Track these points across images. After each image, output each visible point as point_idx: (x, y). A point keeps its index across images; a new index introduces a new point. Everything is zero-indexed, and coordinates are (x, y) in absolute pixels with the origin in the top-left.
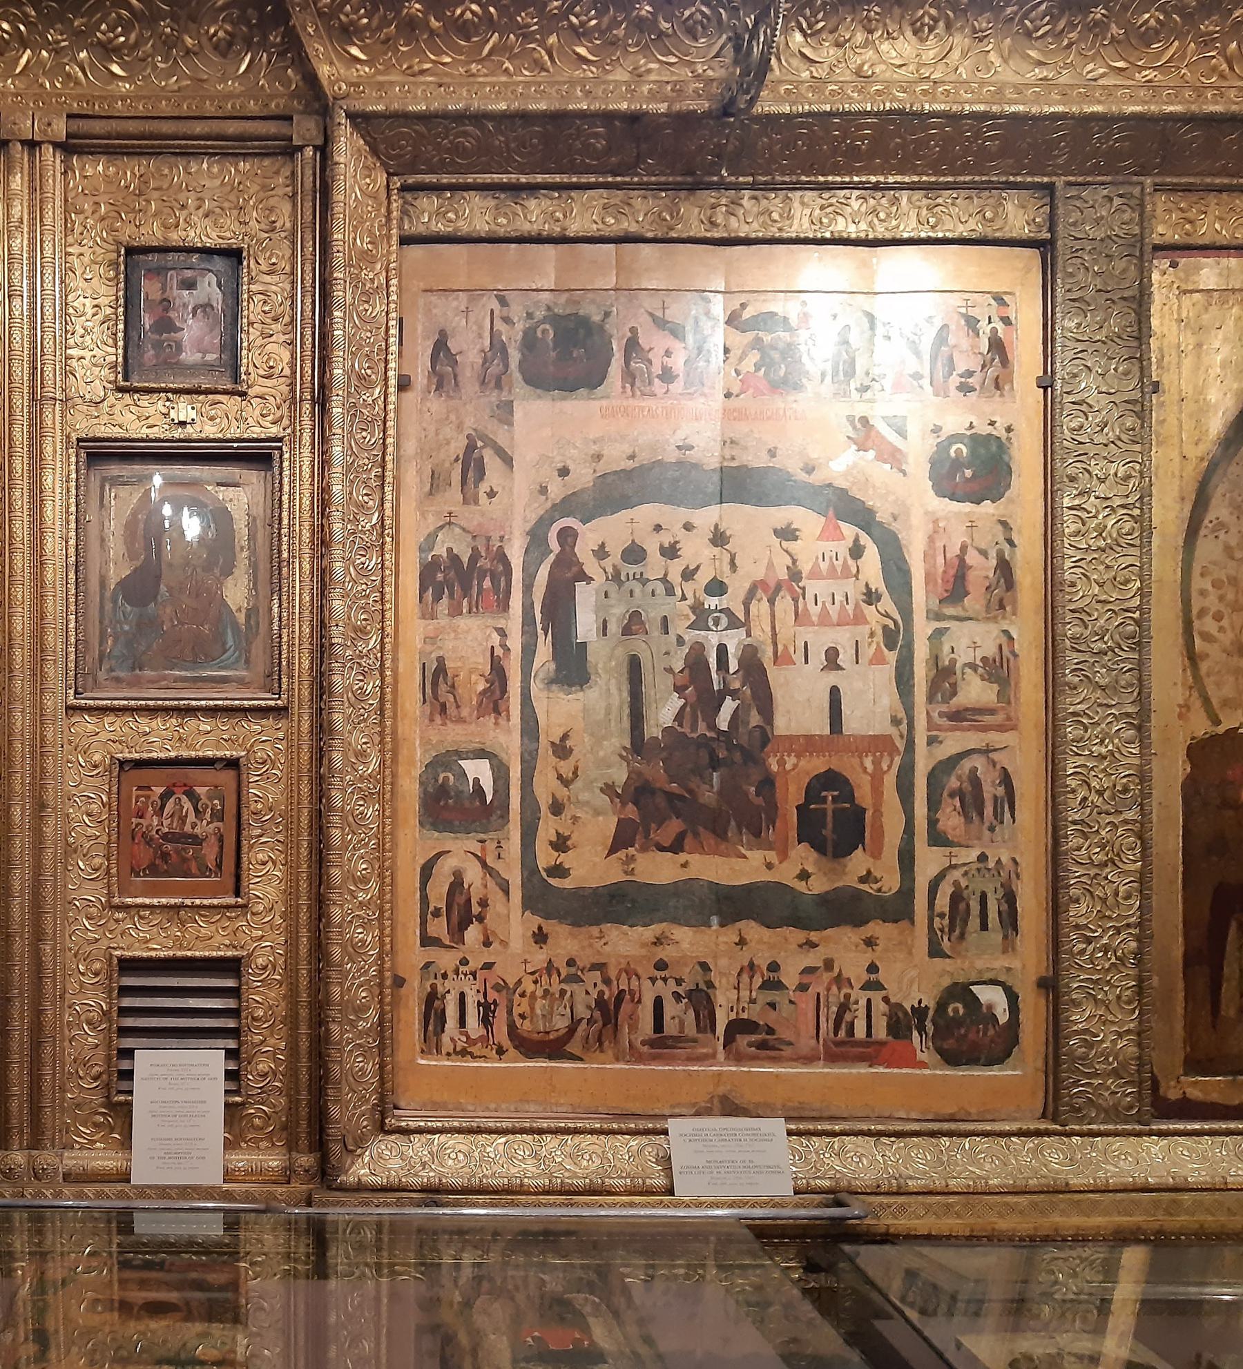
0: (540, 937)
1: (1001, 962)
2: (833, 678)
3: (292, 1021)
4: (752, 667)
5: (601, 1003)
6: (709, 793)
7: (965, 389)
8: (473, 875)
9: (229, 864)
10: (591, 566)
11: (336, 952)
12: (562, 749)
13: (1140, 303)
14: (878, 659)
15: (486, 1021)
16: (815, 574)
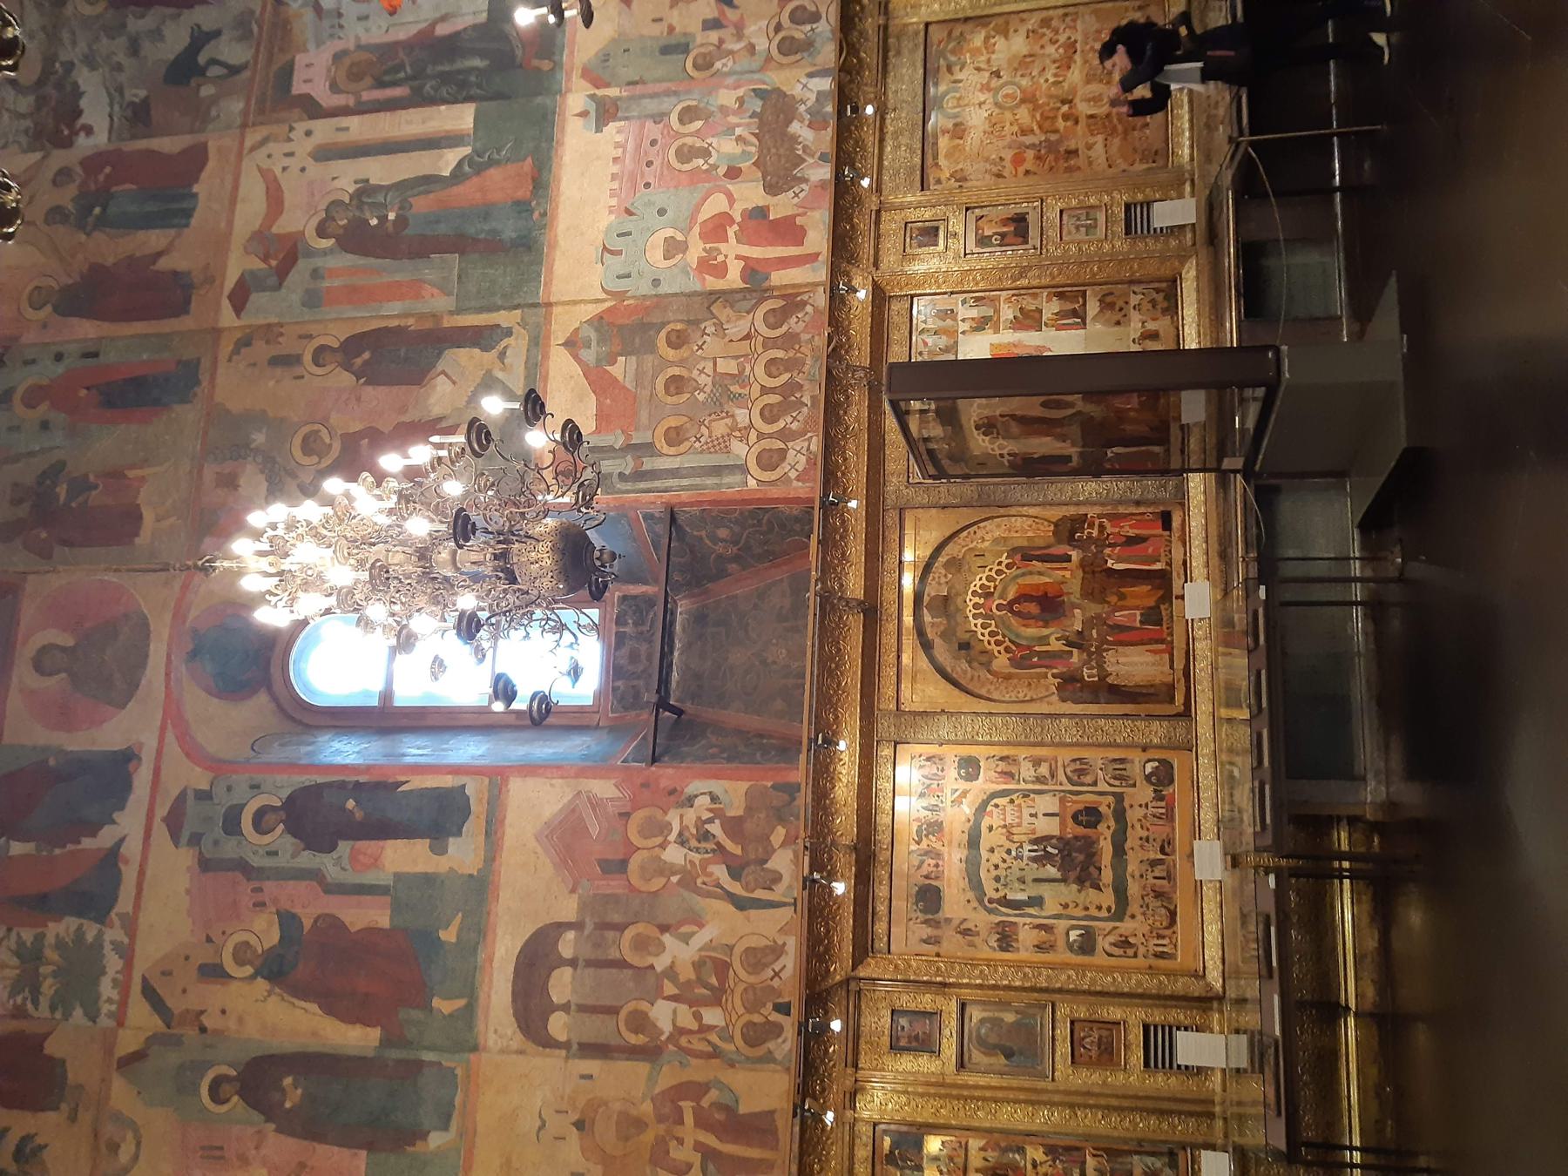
0: (1133, 917)
1: (1137, 762)
2: (1040, 816)
3: (1165, 1007)
4: (1035, 841)
5: (1156, 897)
6: (1081, 857)
7: (943, 770)
8: (1111, 939)
9: (1109, 1026)
10: (1001, 894)
11: (1140, 991)
12: (1066, 906)
13: (915, 714)
14: (1033, 800)
15: (1163, 937)
16: (1004, 820)
